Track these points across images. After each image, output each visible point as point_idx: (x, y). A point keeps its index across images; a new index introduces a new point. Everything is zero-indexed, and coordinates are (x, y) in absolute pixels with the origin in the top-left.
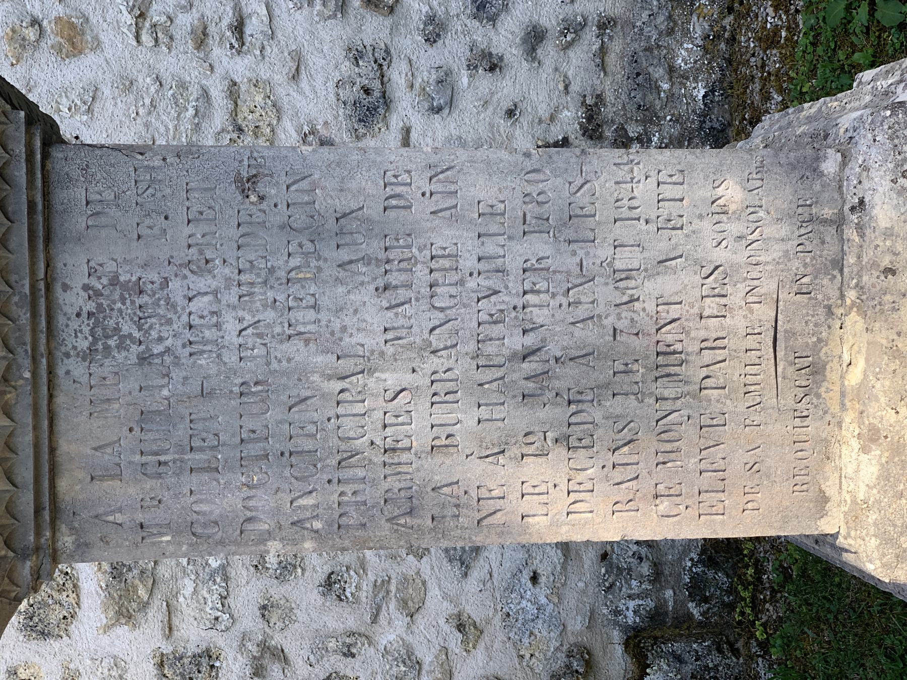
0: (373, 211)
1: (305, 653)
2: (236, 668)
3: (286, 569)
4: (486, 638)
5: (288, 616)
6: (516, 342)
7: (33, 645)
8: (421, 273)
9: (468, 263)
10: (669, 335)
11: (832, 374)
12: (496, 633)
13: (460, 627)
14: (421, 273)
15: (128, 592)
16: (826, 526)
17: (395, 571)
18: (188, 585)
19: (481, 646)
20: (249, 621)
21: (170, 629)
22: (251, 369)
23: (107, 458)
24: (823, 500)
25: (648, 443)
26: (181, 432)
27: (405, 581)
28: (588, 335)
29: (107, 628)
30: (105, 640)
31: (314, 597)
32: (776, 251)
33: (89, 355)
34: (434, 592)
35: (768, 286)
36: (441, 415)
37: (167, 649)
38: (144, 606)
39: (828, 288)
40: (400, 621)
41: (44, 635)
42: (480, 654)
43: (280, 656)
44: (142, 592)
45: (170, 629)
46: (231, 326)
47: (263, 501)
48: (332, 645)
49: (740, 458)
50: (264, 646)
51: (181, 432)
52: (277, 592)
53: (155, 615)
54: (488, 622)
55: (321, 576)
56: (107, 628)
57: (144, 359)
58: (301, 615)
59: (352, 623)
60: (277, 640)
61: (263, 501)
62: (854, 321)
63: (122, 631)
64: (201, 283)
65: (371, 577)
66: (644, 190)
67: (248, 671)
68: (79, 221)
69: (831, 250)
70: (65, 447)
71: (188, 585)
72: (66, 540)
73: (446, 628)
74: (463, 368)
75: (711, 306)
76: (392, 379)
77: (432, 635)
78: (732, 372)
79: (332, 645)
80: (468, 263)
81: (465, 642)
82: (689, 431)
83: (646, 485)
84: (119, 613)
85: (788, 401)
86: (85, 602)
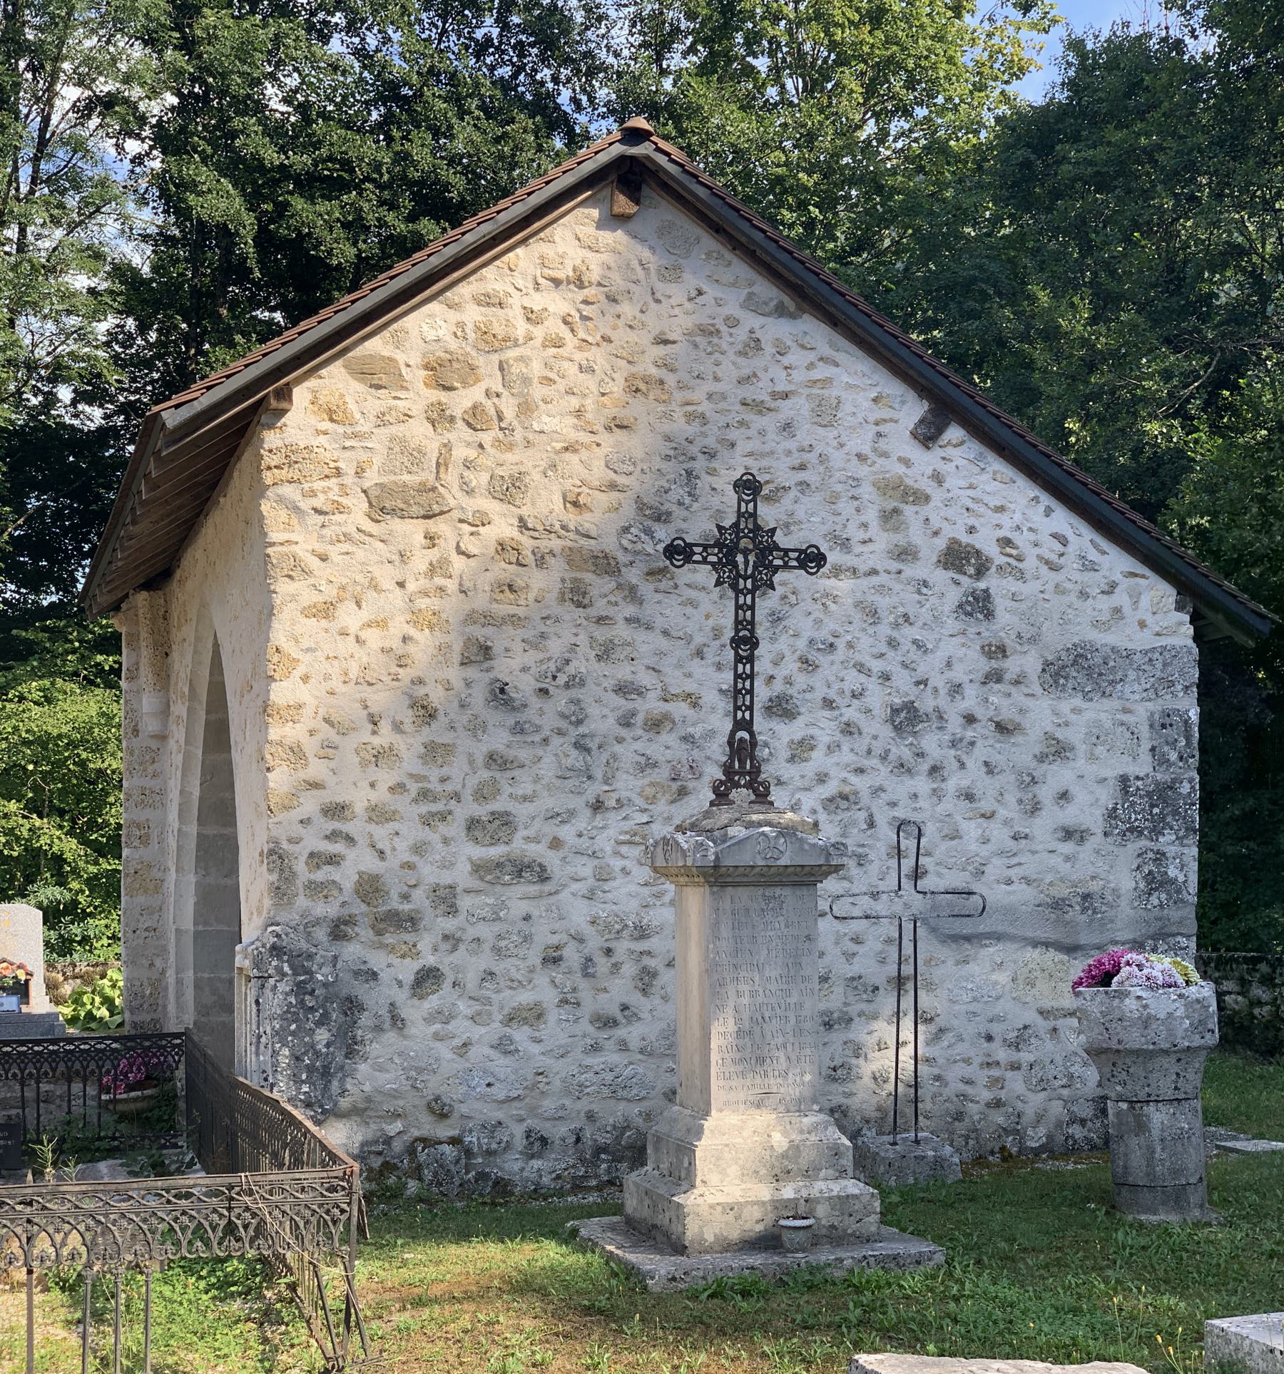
0: (802, 973)
1: (455, 962)
2: (448, 926)
3: (497, 951)
4: (459, 1059)
5: (474, 953)
6: (767, 1015)
7: (463, 823)
8: (785, 987)
9: (788, 1000)
10: (768, 1060)
11: (758, 1111)
12: (461, 1064)
13: (465, 1045)
14: (785, 987)
15: (489, 871)
16: (713, 1112)
17: (494, 1009)
18: (491, 901)
19: (455, 1056)
20: (472, 932)
21: (467, 891)
22: (760, 940)
23: (737, 900)
24: (721, 1111)
25: (738, 1056)
26: (743, 920)
27: (490, 1014)
28: (769, 1036)
29: (470, 859)
30: (464, 859)
31: (483, 967)
32: (792, 1092)
33: (764, 895)
34: (483, 1030)
35: (782, 1090)
36: (747, 993)
37: (459, 890)
38: (482, 879)
39: (782, 1108)
40: (469, 1012)
41: (469, 829)
42: (450, 1056)
43: (454, 949)
44: (489, 878)
45: (467, 891)
46: (771, 933)
47: (725, 943)
48: (460, 976)
49: (733, 1084)
50: (459, 940)
51: (743, 920)
52: (486, 947)
53: (476, 884)
54: (467, 1060)
55: (495, 969)
56: (470, 859)
57: (763, 910)
58: (474, 959)
59: (469, 986)
60: (462, 947)
61: (725, 943)
62: (774, 1116)
63: (469, 867)
64: (783, 926)
65: (493, 996)
66: (808, 1052)
67: (447, 932)
68: (798, 893)
69: (792, 1109)
70: (740, 889)
71: (491, 901)
72: (715, 889)
73: (465, 1037)
74: (760, 999)
75: (776, 1073)
76: (757, 979)
77: (461, 1029)
78: (758, 1080)
79: (460, 976)
80: (788, 1000)
81: (458, 1048)
82: (740, 1068)
83: (727, 1056)
84: (479, 866)
85: (751, 1098)
86: (484, 849)
